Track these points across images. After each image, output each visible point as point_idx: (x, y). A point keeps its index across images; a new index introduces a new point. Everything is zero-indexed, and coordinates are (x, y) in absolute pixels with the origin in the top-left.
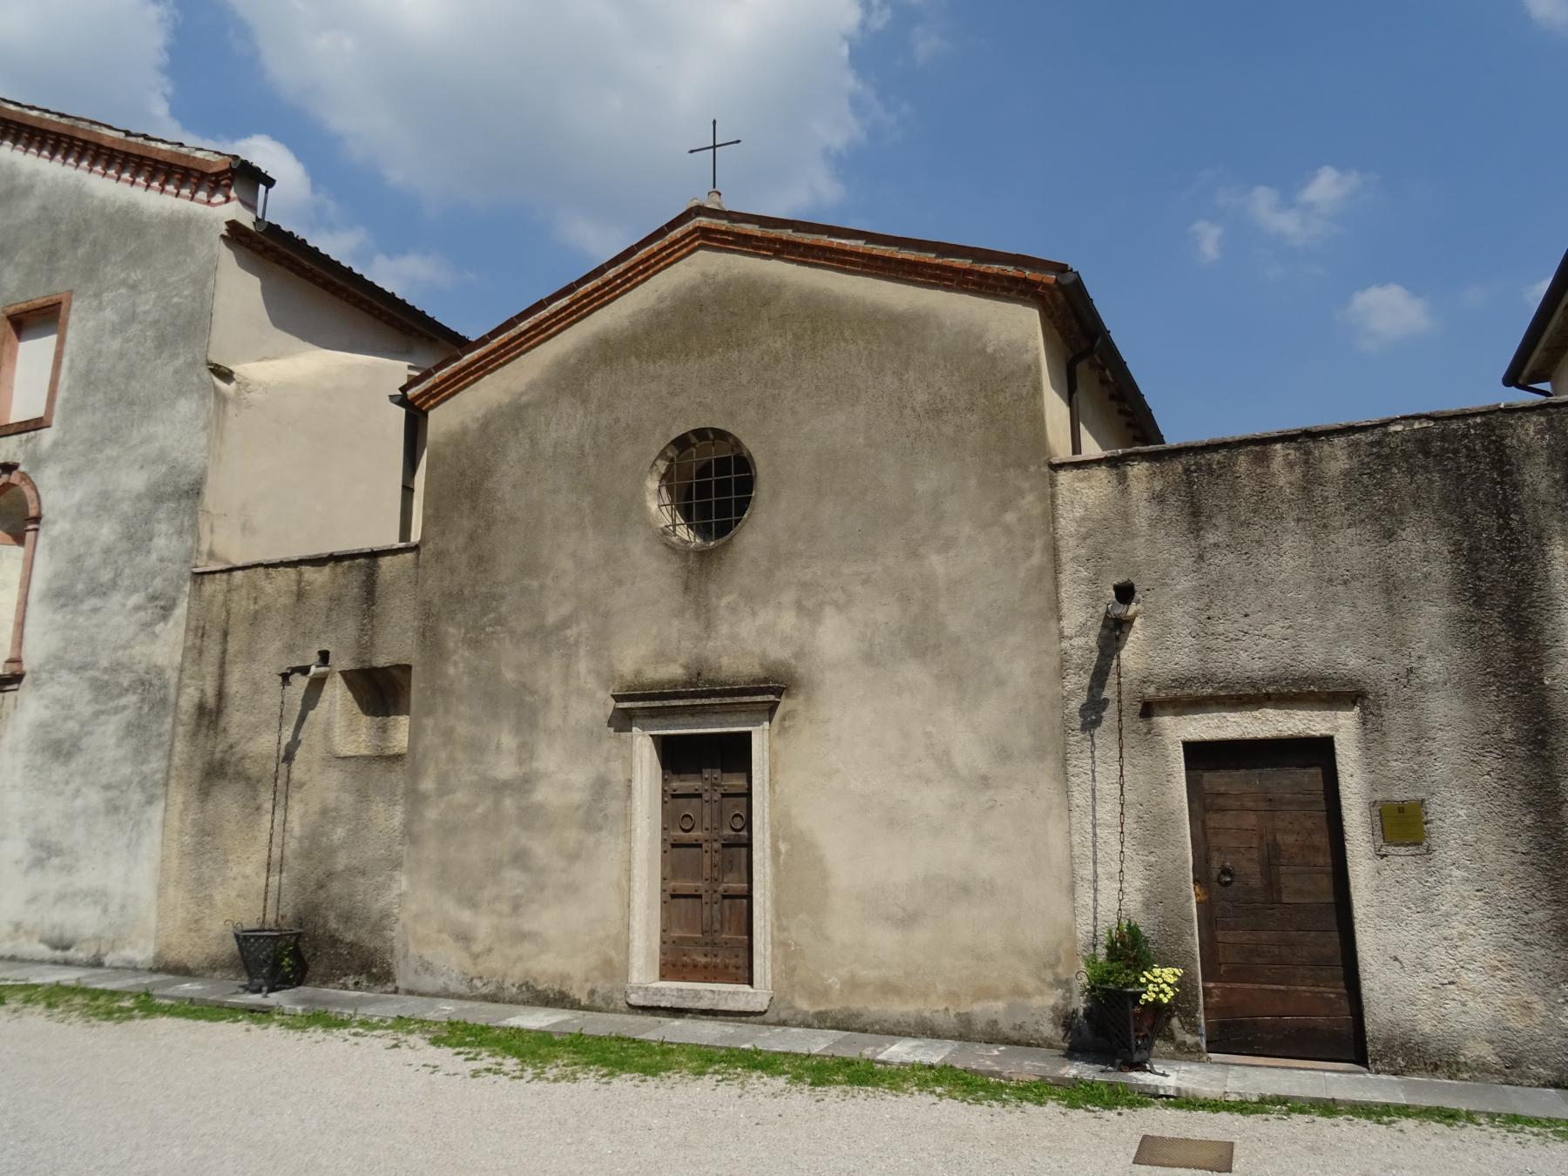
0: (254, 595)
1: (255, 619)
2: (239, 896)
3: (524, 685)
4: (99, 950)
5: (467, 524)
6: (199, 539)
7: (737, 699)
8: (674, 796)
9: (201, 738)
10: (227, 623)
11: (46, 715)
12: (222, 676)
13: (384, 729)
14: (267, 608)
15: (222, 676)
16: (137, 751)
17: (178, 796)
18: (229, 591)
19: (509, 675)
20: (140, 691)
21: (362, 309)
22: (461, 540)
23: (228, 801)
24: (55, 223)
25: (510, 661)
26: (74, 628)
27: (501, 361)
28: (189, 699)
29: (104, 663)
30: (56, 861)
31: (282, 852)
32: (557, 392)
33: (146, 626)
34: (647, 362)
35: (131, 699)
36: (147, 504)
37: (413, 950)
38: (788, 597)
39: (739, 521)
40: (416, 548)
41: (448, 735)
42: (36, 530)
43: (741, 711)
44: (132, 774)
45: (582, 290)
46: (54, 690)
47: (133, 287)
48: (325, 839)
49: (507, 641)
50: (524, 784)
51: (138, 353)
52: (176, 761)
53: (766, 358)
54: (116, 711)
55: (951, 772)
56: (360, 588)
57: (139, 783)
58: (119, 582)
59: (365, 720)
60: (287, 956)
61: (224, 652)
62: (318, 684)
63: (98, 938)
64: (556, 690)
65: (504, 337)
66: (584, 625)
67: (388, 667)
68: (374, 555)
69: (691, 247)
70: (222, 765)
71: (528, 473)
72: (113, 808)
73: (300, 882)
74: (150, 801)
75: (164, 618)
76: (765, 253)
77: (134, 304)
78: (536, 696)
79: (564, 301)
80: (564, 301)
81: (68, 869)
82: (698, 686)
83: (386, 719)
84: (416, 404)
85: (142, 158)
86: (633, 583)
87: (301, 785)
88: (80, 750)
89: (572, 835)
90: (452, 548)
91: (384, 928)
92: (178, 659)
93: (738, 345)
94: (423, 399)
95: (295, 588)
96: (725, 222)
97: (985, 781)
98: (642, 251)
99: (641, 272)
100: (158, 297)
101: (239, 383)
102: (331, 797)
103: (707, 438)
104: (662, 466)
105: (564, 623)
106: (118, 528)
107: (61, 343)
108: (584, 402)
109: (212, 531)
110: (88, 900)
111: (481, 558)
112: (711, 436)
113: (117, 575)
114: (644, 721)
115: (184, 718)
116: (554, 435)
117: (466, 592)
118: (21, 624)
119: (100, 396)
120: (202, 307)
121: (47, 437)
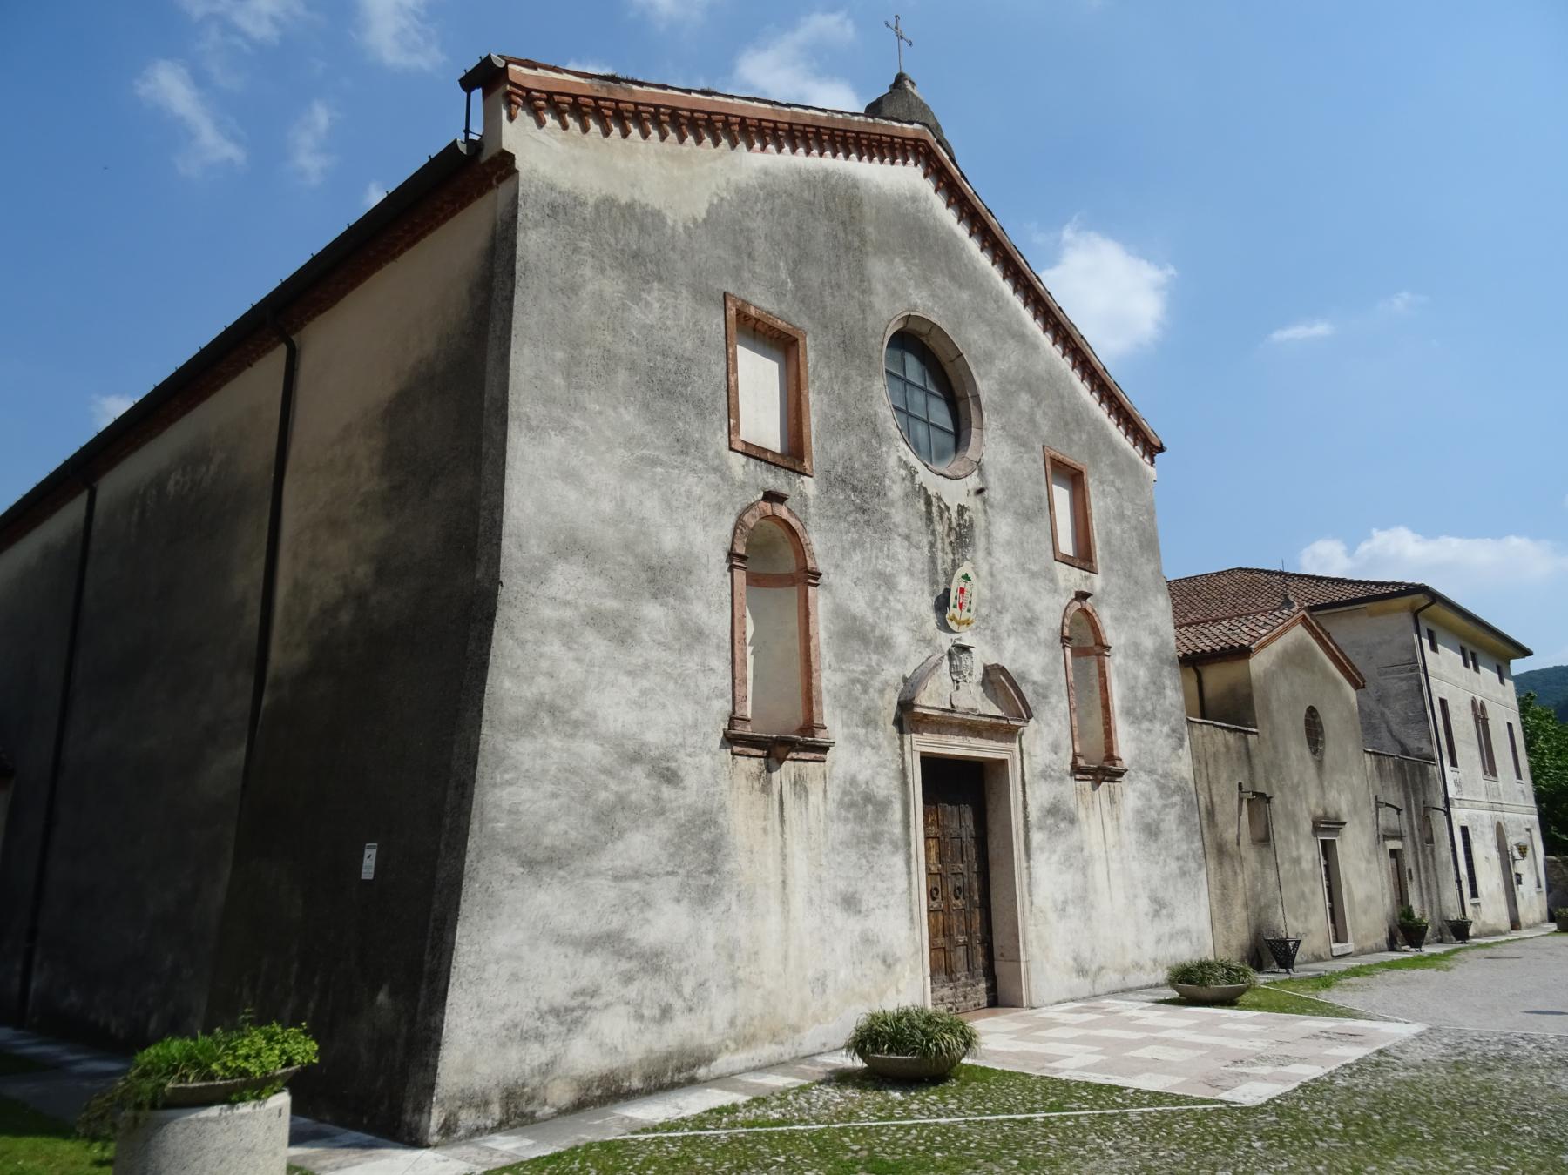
11: (1139, 804)
17: (1212, 864)
29: (1160, 771)
30: (1164, 912)
54: (1173, 805)
72: (1183, 873)
81: (1171, 916)
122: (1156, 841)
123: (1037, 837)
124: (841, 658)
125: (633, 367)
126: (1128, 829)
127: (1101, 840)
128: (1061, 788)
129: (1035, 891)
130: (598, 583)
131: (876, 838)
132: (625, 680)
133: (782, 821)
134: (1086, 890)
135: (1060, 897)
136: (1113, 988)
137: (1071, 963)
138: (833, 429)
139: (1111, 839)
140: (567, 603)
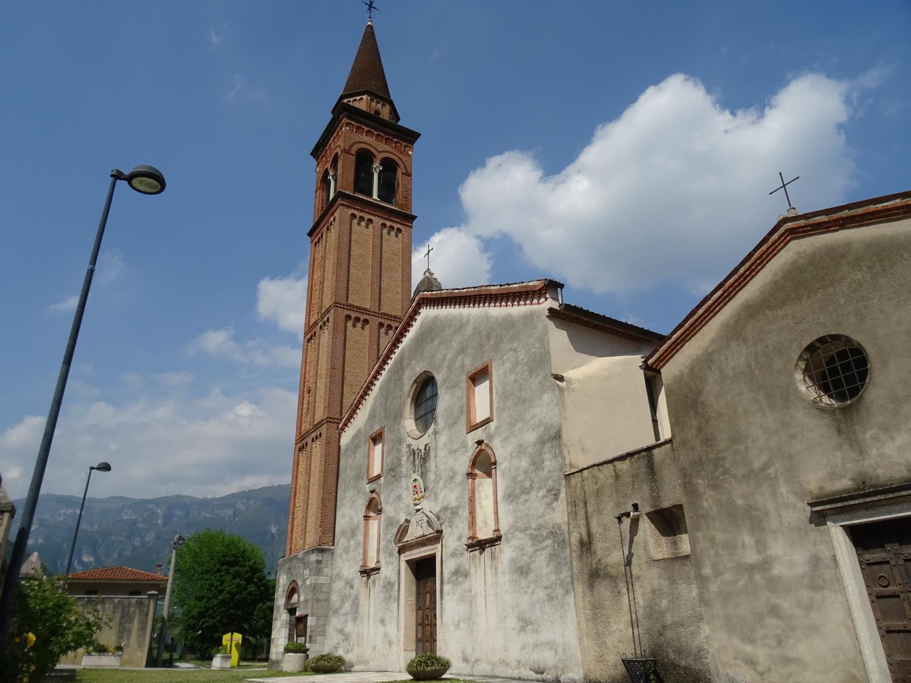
0: (595, 481)
1: (598, 493)
2: (619, 641)
3: (750, 506)
4: (557, 674)
5: (694, 423)
6: (564, 458)
7: (896, 494)
8: (869, 564)
9: (584, 558)
10: (585, 497)
11: (514, 554)
12: (588, 525)
13: (675, 543)
14: (603, 486)
15: (588, 525)
16: (556, 568)
17: (580, 589)
18: (583, 481)
19: (739, 502)
20: (552, 537)
21: (613, 334)
22: (694, 431)
23: (603, 589)
24: (480, 333)
25: (738, 493)
26: (518, 511)
27: (692, 333)
28: (575, 539)
29: (534, 526)
30: (530, 627)
31: (636, 615)
32: (728, 341)
34: (776, 310)
35: (549, 542)
36: (539, 446)
37: (721, 671)
39: (864, 384)
40: (669, 441)
41: (712, 540)
42: (495, 468)
43: (902, 502)
44: (556, 579)
45: (728, 284)
46: (515, 542)
47: (515, 350)
48: (657, 607)
49: (733, 482)
50: (765, 565)
51: (522, 378)
52: (575, 571)
53: (853, 286)
54: (544, 549)
56: (646, 468)
57: (560, 584)
58: (534, 486)
59: (664, 539)
60: (652, 673)
61: (586, 512)
62: (635, 522)
63: (555, 667)
64: (770, 506)
65: (691, 321)
66: (778, 465)
67: (670, 507)
68: (649, 449)
69: (786, 241)
70: (597, 571)
71: (722, 388)
72: (551, 598)
73: (649, 632)
74: (567, 593)
75: (556, 499)
76: (833, 228)
77: (517, 358)
78: (759, 512)
79: (719, 293)
80: (719, 293)
81: (536, 631)
82: (865, 490)
83: (675, 538)
84: (654, 367)
85: (508, 294)
86: (803, 435)
87: (639, 578)
88: (531, 570)
89: (805, 594)
90: (690, 437)
91: (702, 658)
92: (566, 519)
93: (832, 284)
94: (657, 363)
95: (613, 474)
96: (803, 221)
98: (757, 253)
99: (759, 264)
100: (526, 351)
101: (567, 381)
102: (655, 583)
103: (827, 342)
104: (802, 365)
105: (765, 467)
106: (528, 460)
107: (491, 383)
108: (745, 342)
109: (569, 454)
110: (548, 647)
111: (707, 439)
112: (830, 340)
113: (532, 482)
114: (834, 517)
115: (574, 548)
116: (732, 364)
117: (703, 459)
118: (496, 513)
119: (511, 402)
120: (545, 350)
121: (492, 425)
122: (526, 577)
123: (447, 588)
126: (503, 573)
127: (483, 583)
128: (461, 559)
129: (444, 615)
131: (390, 597)
134: (471, 614)
135: (457, 618)
136: (485, 673)
137: (460, 654)
139: (489, 582)
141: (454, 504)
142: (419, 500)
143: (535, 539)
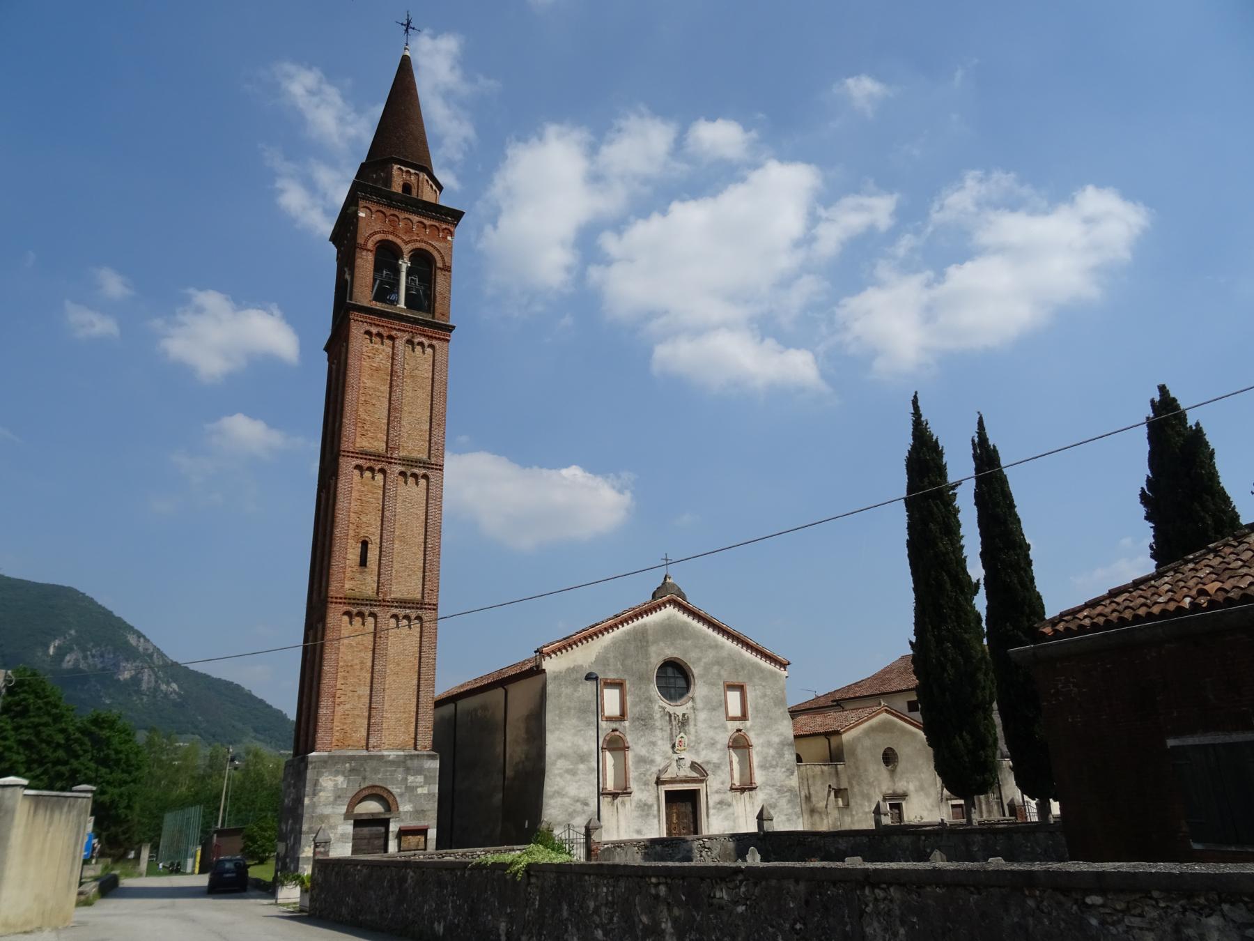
1: (814, 777)
11: (766, 797)
12: (809, 789)
15: (809, 789)
17: (806, 816)
19: (865, 791)
25: (865, 789)
28: (803, 794)
29: (779, 785)
33: (788, 776)
38: (905, 779)
54: (785, 797)
55: (927, 809)
61: (808, 784)
64: (874, 795)
74: (799, 818)
92: (798, 785)
97: (931, 811)
105: (873, 782)
123: (712, 811)
124: (636, 768)
125: (575, 708)
130: (568, 763)
131: (648, 815)
132: (574, 784)
133: (617, 812)
138: (635, 705)
140: (561, 769)
141: (716, 761)
142: (681, 751)
143: (779, 791)
